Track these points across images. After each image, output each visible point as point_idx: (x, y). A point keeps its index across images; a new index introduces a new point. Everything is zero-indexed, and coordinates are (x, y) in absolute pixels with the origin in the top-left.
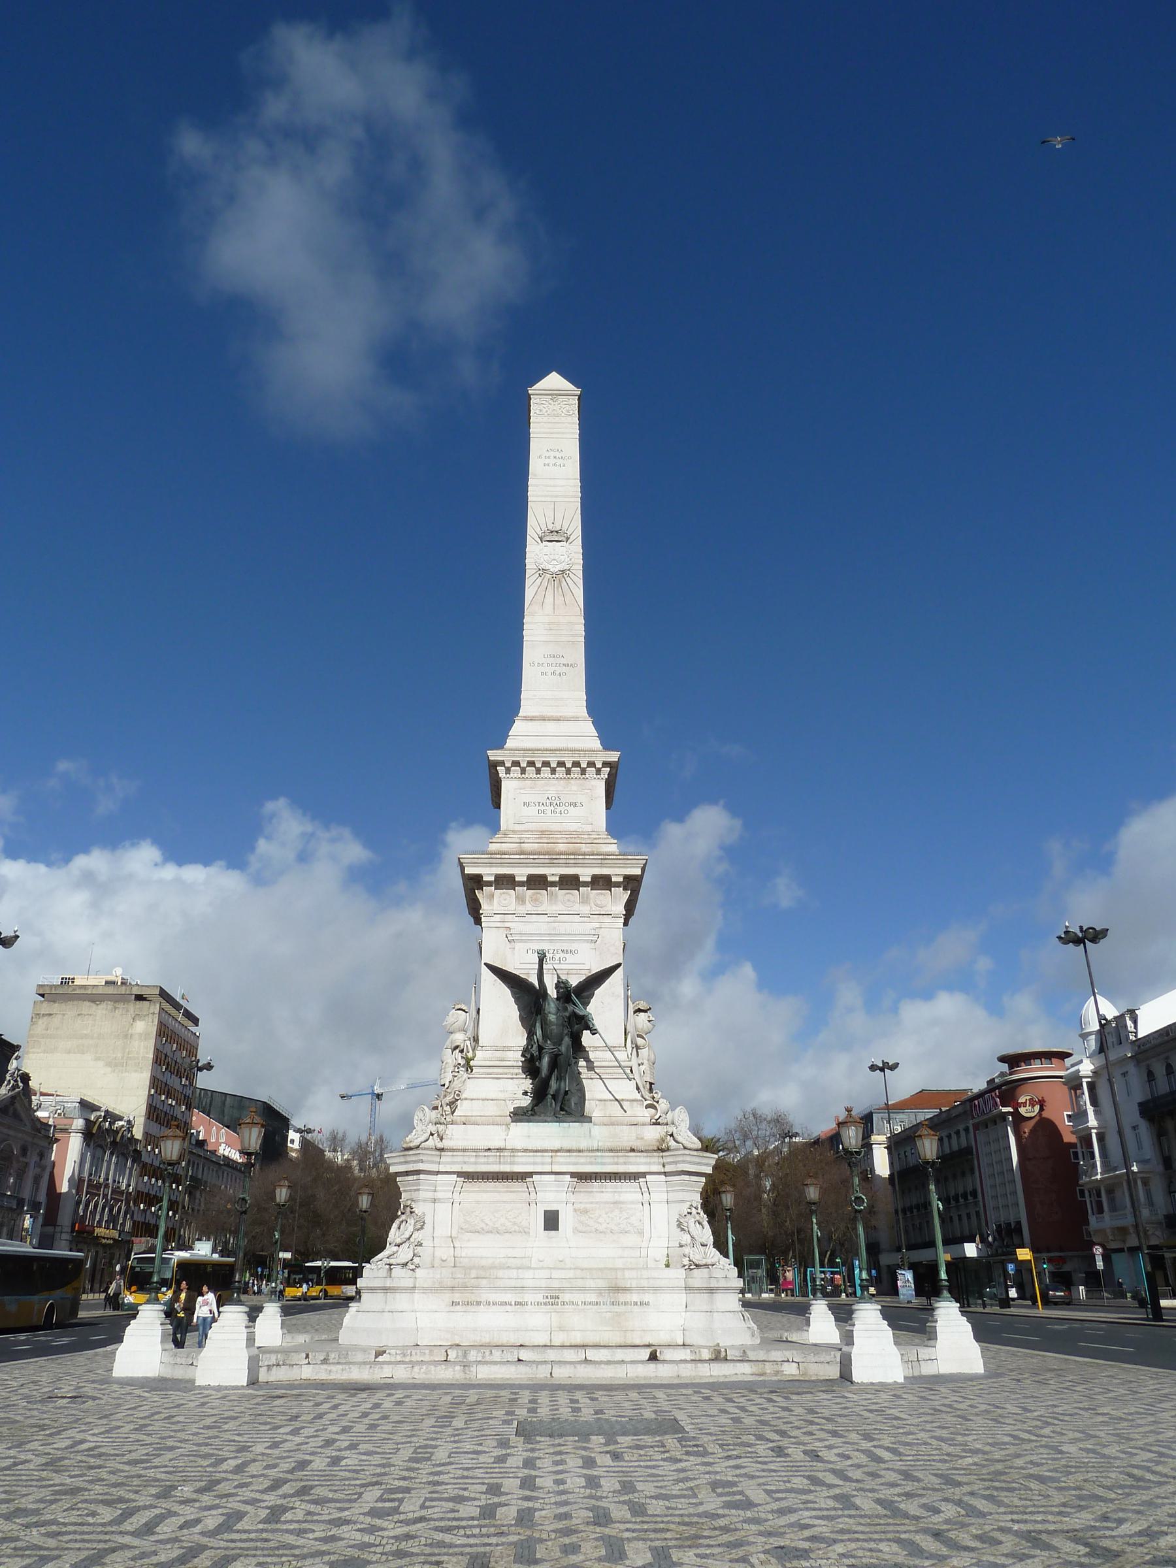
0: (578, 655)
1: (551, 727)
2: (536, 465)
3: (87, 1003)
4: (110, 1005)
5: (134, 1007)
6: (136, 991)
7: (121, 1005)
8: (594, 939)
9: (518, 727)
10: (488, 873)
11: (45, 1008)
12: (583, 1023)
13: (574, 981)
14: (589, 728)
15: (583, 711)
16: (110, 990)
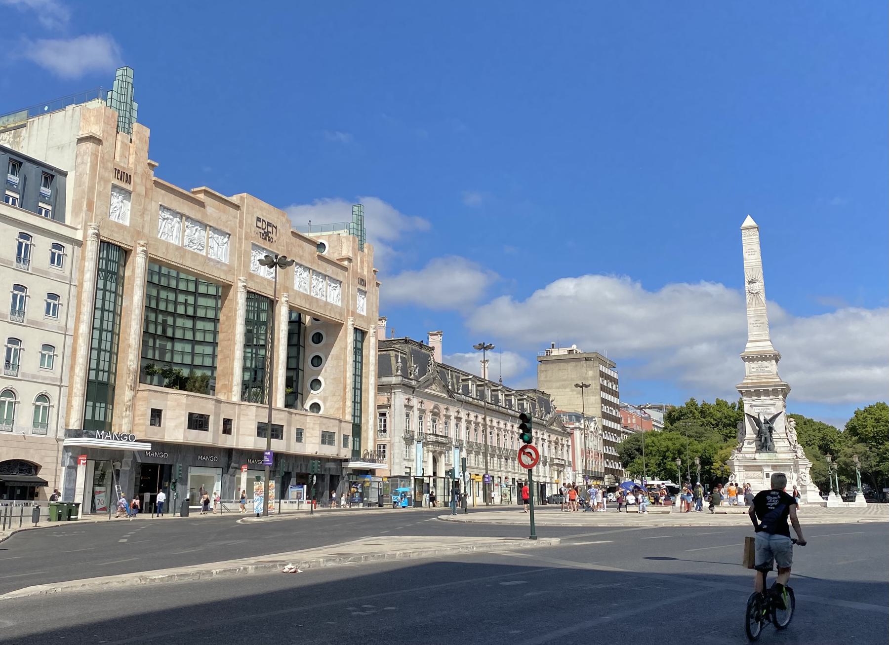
0: (765, 320)
1: (758, 344)
2: (745, 255)
3: (562, 364)
4: (573, 364)
5: (583, 362)
6: (584, 356)
7: (579, 364)
8: (773, 405)
9: (748, 345)
10: (744, 390)
11: (543, 367)
12: (771, 429)
13: (768, 418)
14: (769, 343)
15: (767, 338)
16: (572, 356)
